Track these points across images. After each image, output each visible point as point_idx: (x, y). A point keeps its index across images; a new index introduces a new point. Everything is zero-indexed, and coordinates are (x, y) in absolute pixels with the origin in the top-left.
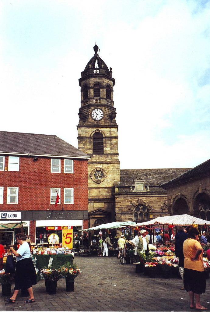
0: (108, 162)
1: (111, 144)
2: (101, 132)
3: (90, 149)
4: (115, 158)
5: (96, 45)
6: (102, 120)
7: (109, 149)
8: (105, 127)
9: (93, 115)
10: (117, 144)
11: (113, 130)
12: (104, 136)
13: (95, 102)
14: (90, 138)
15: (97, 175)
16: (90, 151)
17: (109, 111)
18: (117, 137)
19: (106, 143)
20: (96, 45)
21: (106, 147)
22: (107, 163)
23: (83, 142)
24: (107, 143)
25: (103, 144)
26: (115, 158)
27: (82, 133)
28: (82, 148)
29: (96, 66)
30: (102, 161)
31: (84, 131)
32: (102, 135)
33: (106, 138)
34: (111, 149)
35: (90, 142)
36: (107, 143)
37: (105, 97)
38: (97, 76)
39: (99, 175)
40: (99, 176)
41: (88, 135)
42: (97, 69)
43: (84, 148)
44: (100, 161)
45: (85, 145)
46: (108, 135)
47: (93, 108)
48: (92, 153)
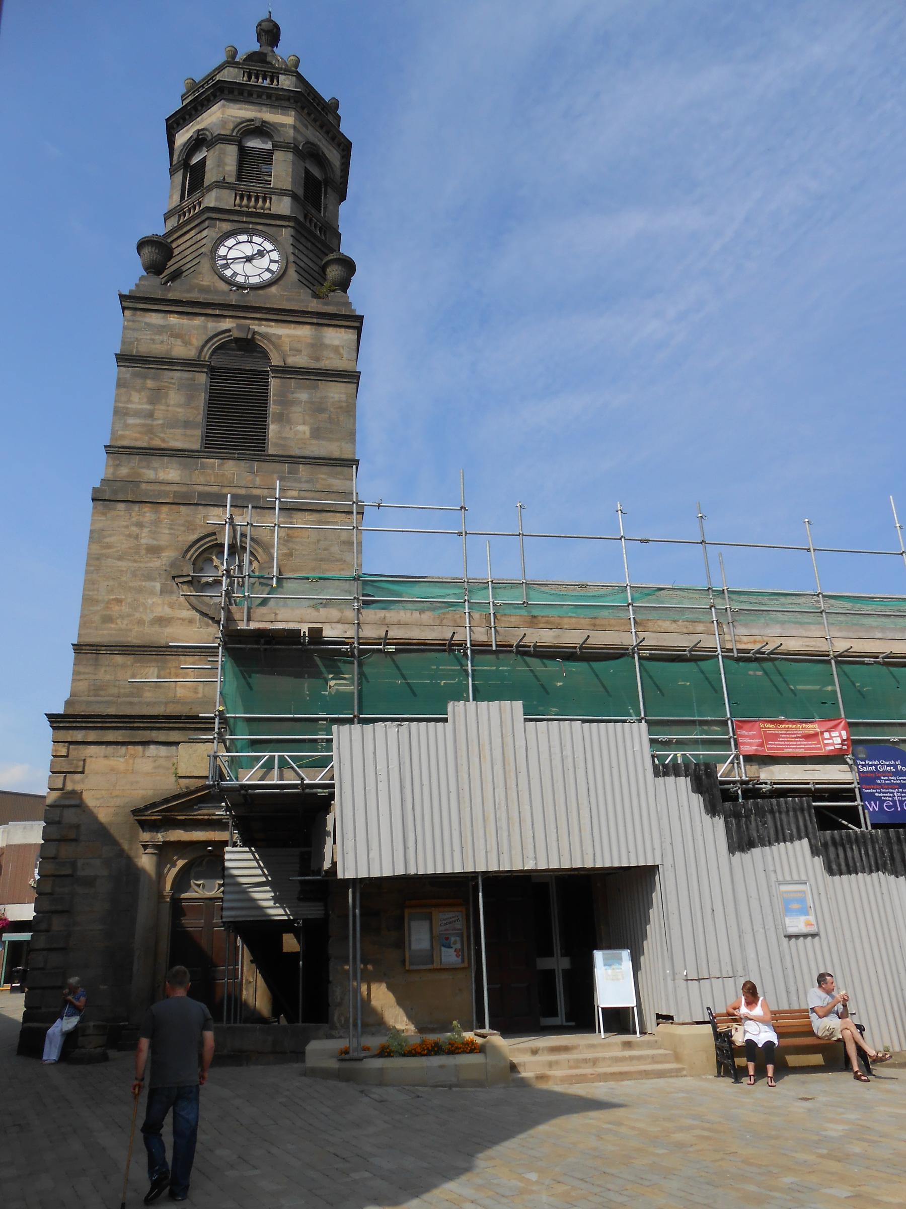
1: (318, 408)
2: (263, 344)
3: (187, 424)
4: (337, 483)
6: (274, 289)
7: (304, 429)
10: (350, 410)
11: (337, 337)
12: (276, 360)
14: (188, 364)
16: (189, 432)
17: (311, 255)
18: (352, 377)
19: (285, 403)
21: (281, 418)
23: (150, 383)
24: (293, 403)
26: (337, 483)
27: (146, 336)
28: (137, 414)
31: (161, 329)
32: (265, 355)
34: (316, 433)
35: (190, 389)
36: (298, 402)
41: (180, 350)
43: (151, 415)
45: (156, 396)
46: (300, 360)
47: (226, 227)
48: (196, 446)
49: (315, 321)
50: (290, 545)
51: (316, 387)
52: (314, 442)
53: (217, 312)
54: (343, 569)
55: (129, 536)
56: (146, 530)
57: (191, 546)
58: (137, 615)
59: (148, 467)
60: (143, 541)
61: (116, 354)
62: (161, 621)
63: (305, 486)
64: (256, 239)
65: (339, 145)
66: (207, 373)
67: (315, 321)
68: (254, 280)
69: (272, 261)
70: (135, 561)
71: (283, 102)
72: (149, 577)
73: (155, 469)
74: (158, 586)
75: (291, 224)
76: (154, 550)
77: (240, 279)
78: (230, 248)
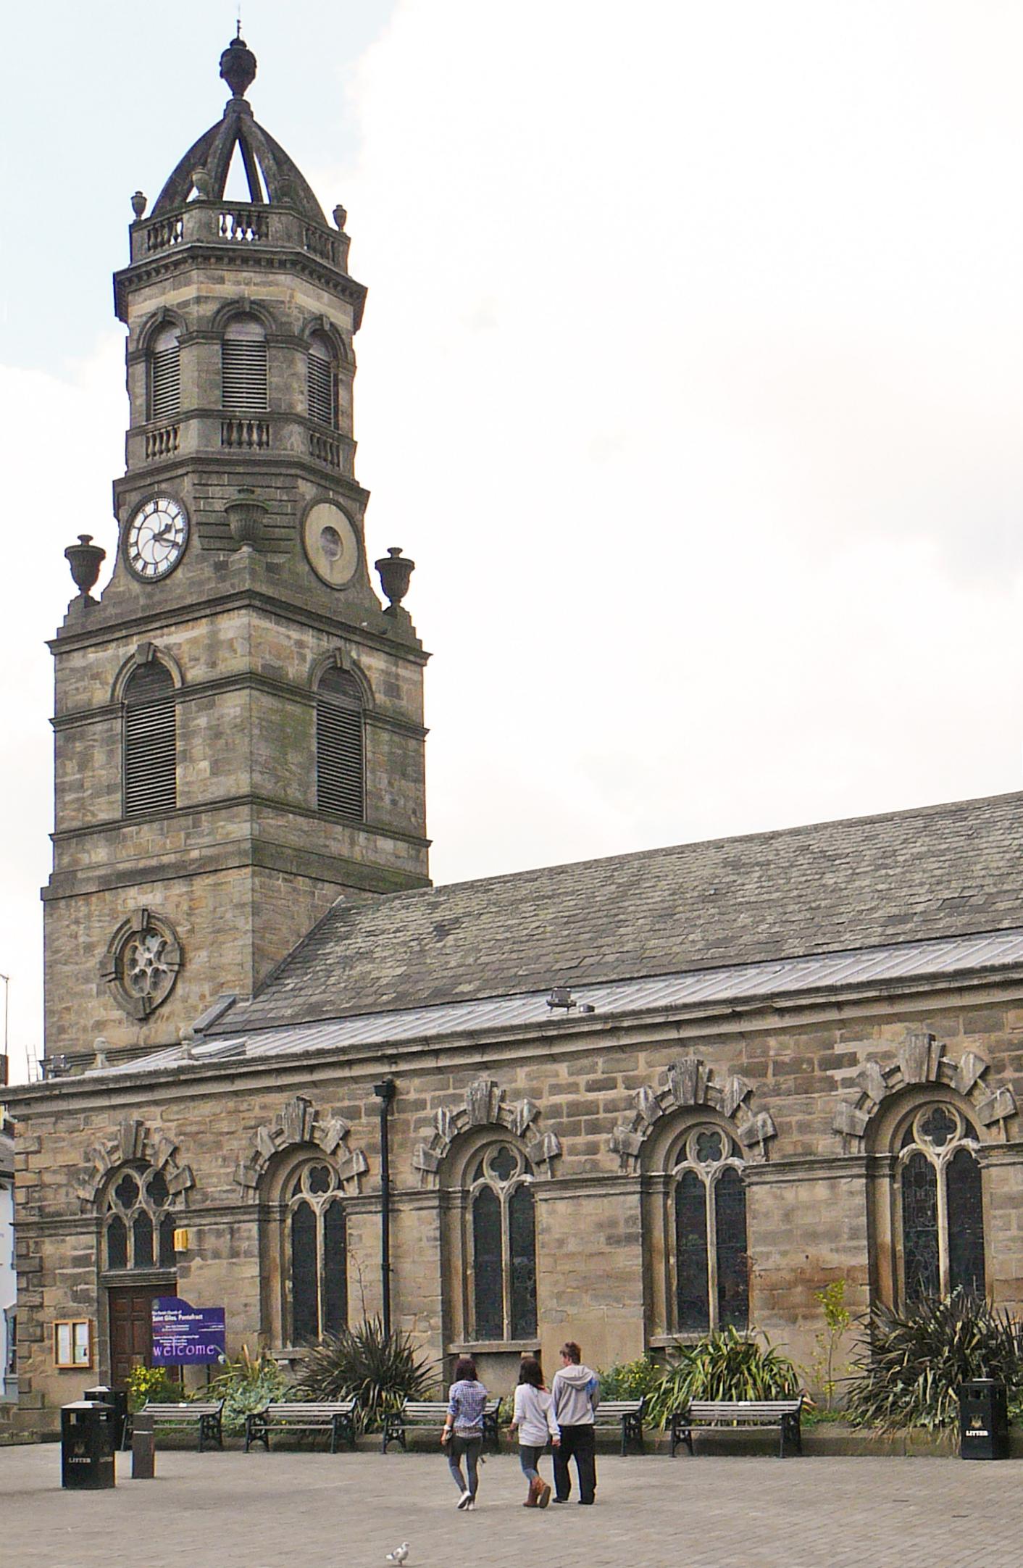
0: (194, 861)
5: (237, 44)
6: (179, 574)
8: (182, 615)
9: (136, 543)
13: (250, 444)
14: (106, 711)
15: (149, 970)
20: (237, 44)
22: (185, 873)
25: (173, 737)
29: (236, 189)
30: (165, 860)
33: (189, 691)
37: (214, 400)
38: (158, 271)
39: (150, 962)
40: (149, 970)
42: (237, 210)
44: (154, 862)
48: (117, 815)
49: (208, 612)
50: (193, 919)
51: (211, 706)
52: (215, 780)
53: (124, 633)
54: (236, 939)
55: (71, 936)
56: (82, 926)
57: (114, 938)
58: (82, 1022)
59: (84, 851)
60: (81, 939)
61: (50, 720)
62: (100, 1026)
63: (206, 840)
64: (163, 504)
65: (282, 264)
66: (122, 717)
67: (208, 612)
68: (163, 567)
69: (177, 531)
70: (77, 964)
71: (182, 267)
72: (87, 980)
73: (88, 852)
74: (94, 987)
75: (190, 469)
76: (89, 948)
77: (150, 571)
78: (140, 529)
